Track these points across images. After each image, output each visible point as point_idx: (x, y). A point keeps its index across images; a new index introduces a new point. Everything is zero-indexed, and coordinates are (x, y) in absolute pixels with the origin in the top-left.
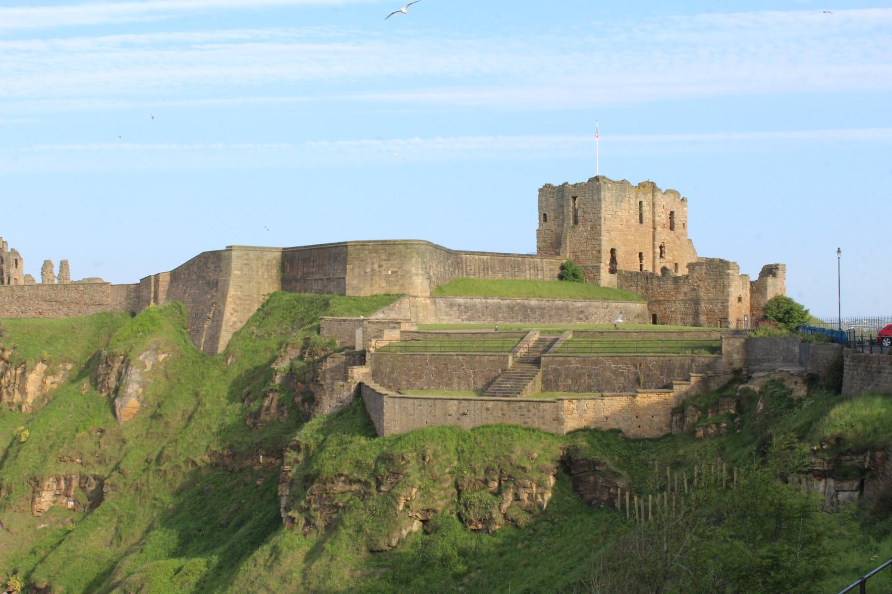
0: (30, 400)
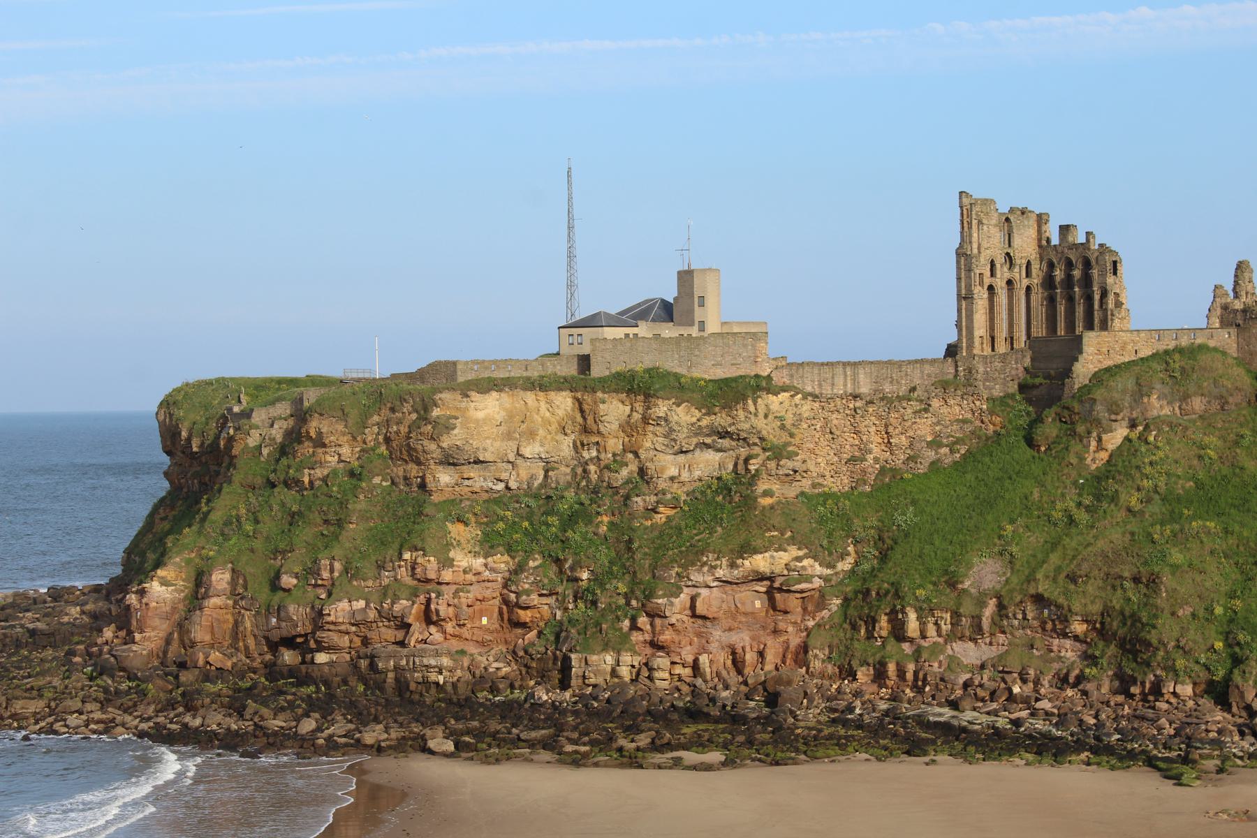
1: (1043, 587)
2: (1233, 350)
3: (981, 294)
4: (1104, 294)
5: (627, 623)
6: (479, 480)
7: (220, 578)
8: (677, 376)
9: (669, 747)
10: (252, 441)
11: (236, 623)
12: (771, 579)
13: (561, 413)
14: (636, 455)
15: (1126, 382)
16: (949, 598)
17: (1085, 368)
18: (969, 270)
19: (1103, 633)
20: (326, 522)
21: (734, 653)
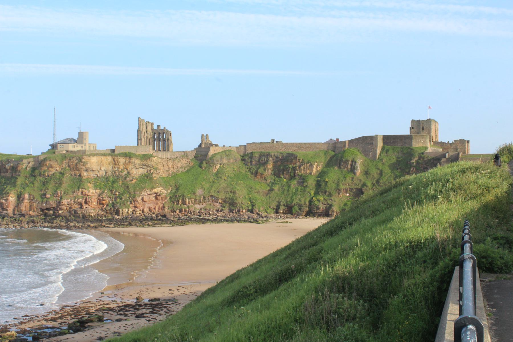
0: (314, 172)
1: (213, 194)
2: (235, 150)
3: (143, 138)
4: (168, 140)
5: (129, 203)
6: (93, 175)
7: (27, 196)
8: (135, 154)
9: (156, 224)
10: (24, 166)
11: (31, 206)
12: (156, 194)
13: (109, 161)
14: (127, 169)
15: (218, 157)
16: (194, 196)
17: (211, 154)
18: (141, 134)
19: (225, 202)
20: (56, 183)
21: (150, 208)
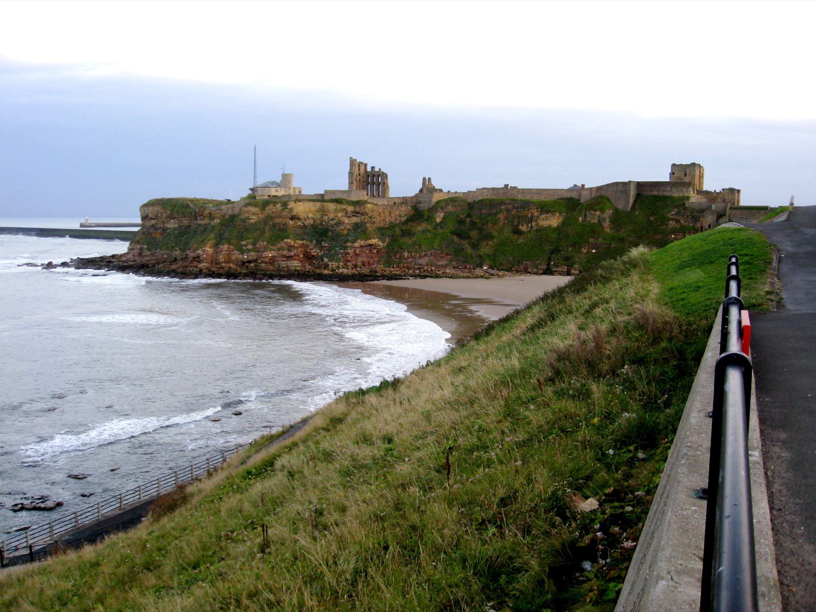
4: (384, 184)
21: (363, 262)
